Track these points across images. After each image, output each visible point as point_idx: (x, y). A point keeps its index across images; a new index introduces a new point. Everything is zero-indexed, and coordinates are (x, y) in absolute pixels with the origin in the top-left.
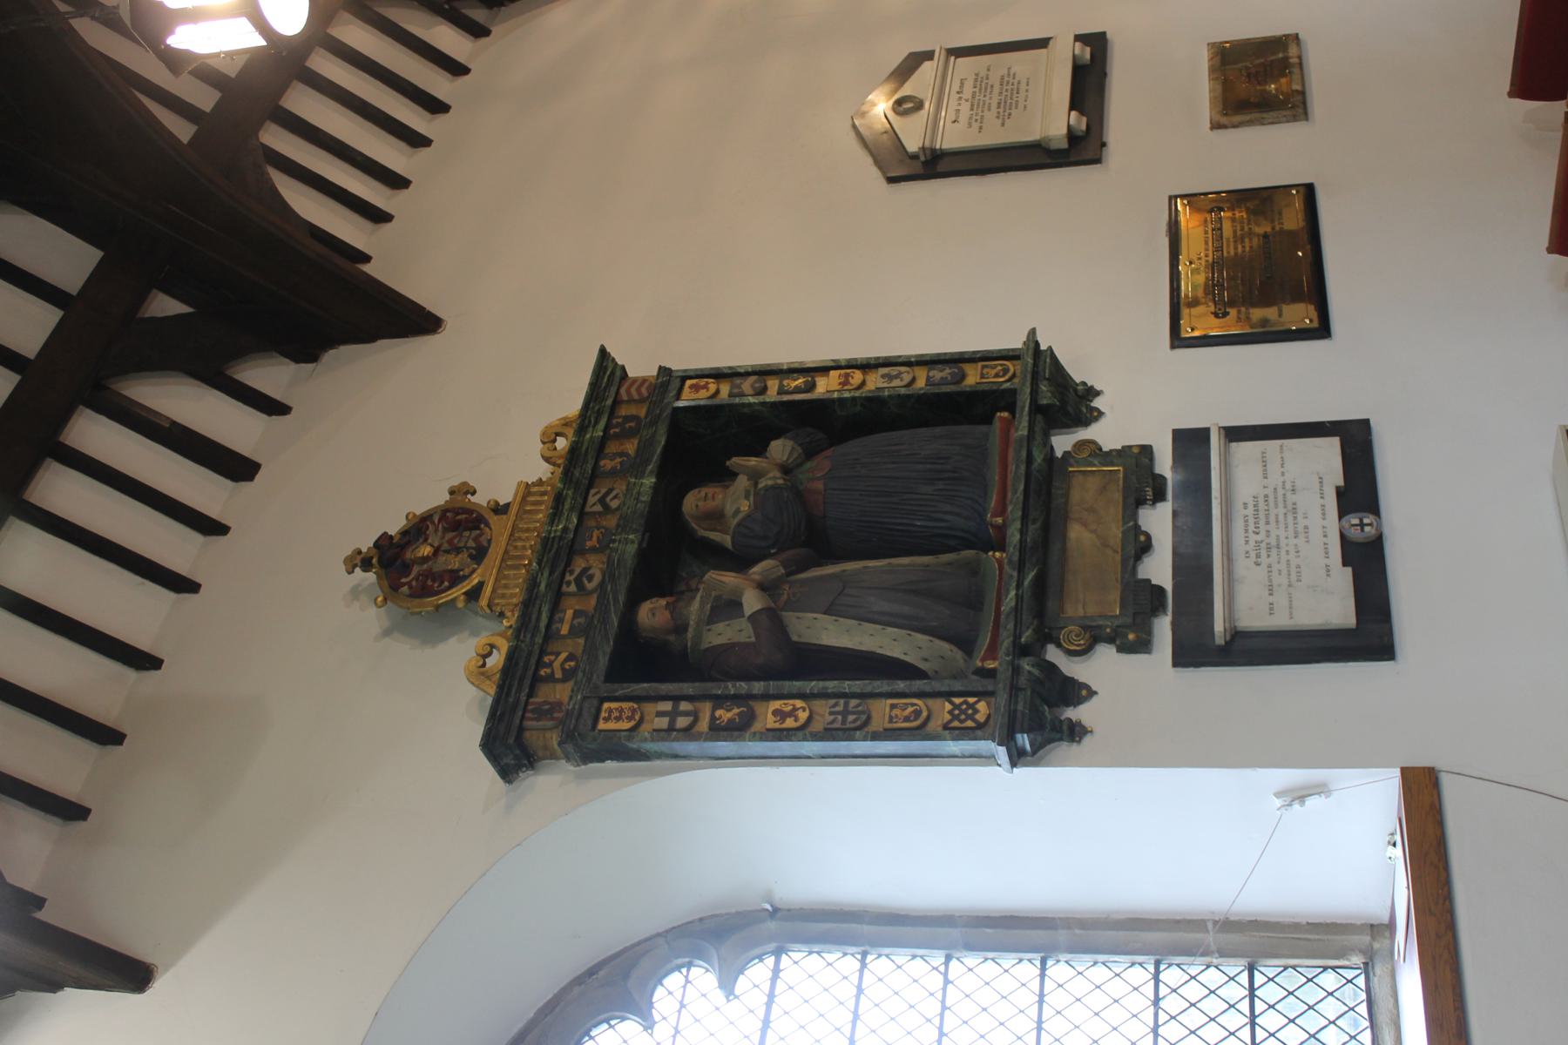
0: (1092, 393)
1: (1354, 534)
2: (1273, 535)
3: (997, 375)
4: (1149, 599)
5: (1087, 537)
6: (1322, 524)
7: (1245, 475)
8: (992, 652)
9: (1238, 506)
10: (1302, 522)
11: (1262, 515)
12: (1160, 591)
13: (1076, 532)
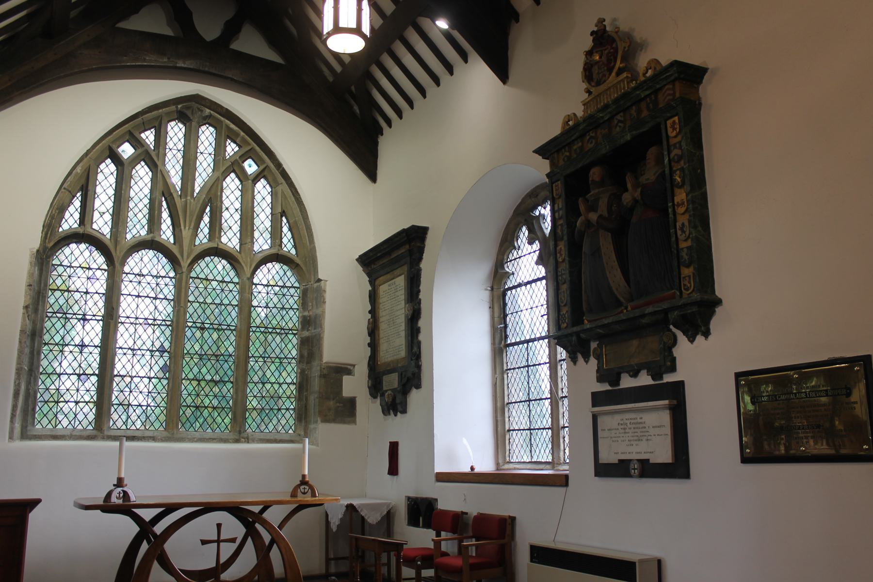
0: (707, 334)
1: (632, 466)
2: (630, 431)
3: (685, 285)
4: (615, 380)
5: (635, 349)
7: (656, 418)
8: (589, 321)
9: (641, 415)
10: (634, 443)
11: (638, 426)
12: (619, 385)
13: (635, 343)
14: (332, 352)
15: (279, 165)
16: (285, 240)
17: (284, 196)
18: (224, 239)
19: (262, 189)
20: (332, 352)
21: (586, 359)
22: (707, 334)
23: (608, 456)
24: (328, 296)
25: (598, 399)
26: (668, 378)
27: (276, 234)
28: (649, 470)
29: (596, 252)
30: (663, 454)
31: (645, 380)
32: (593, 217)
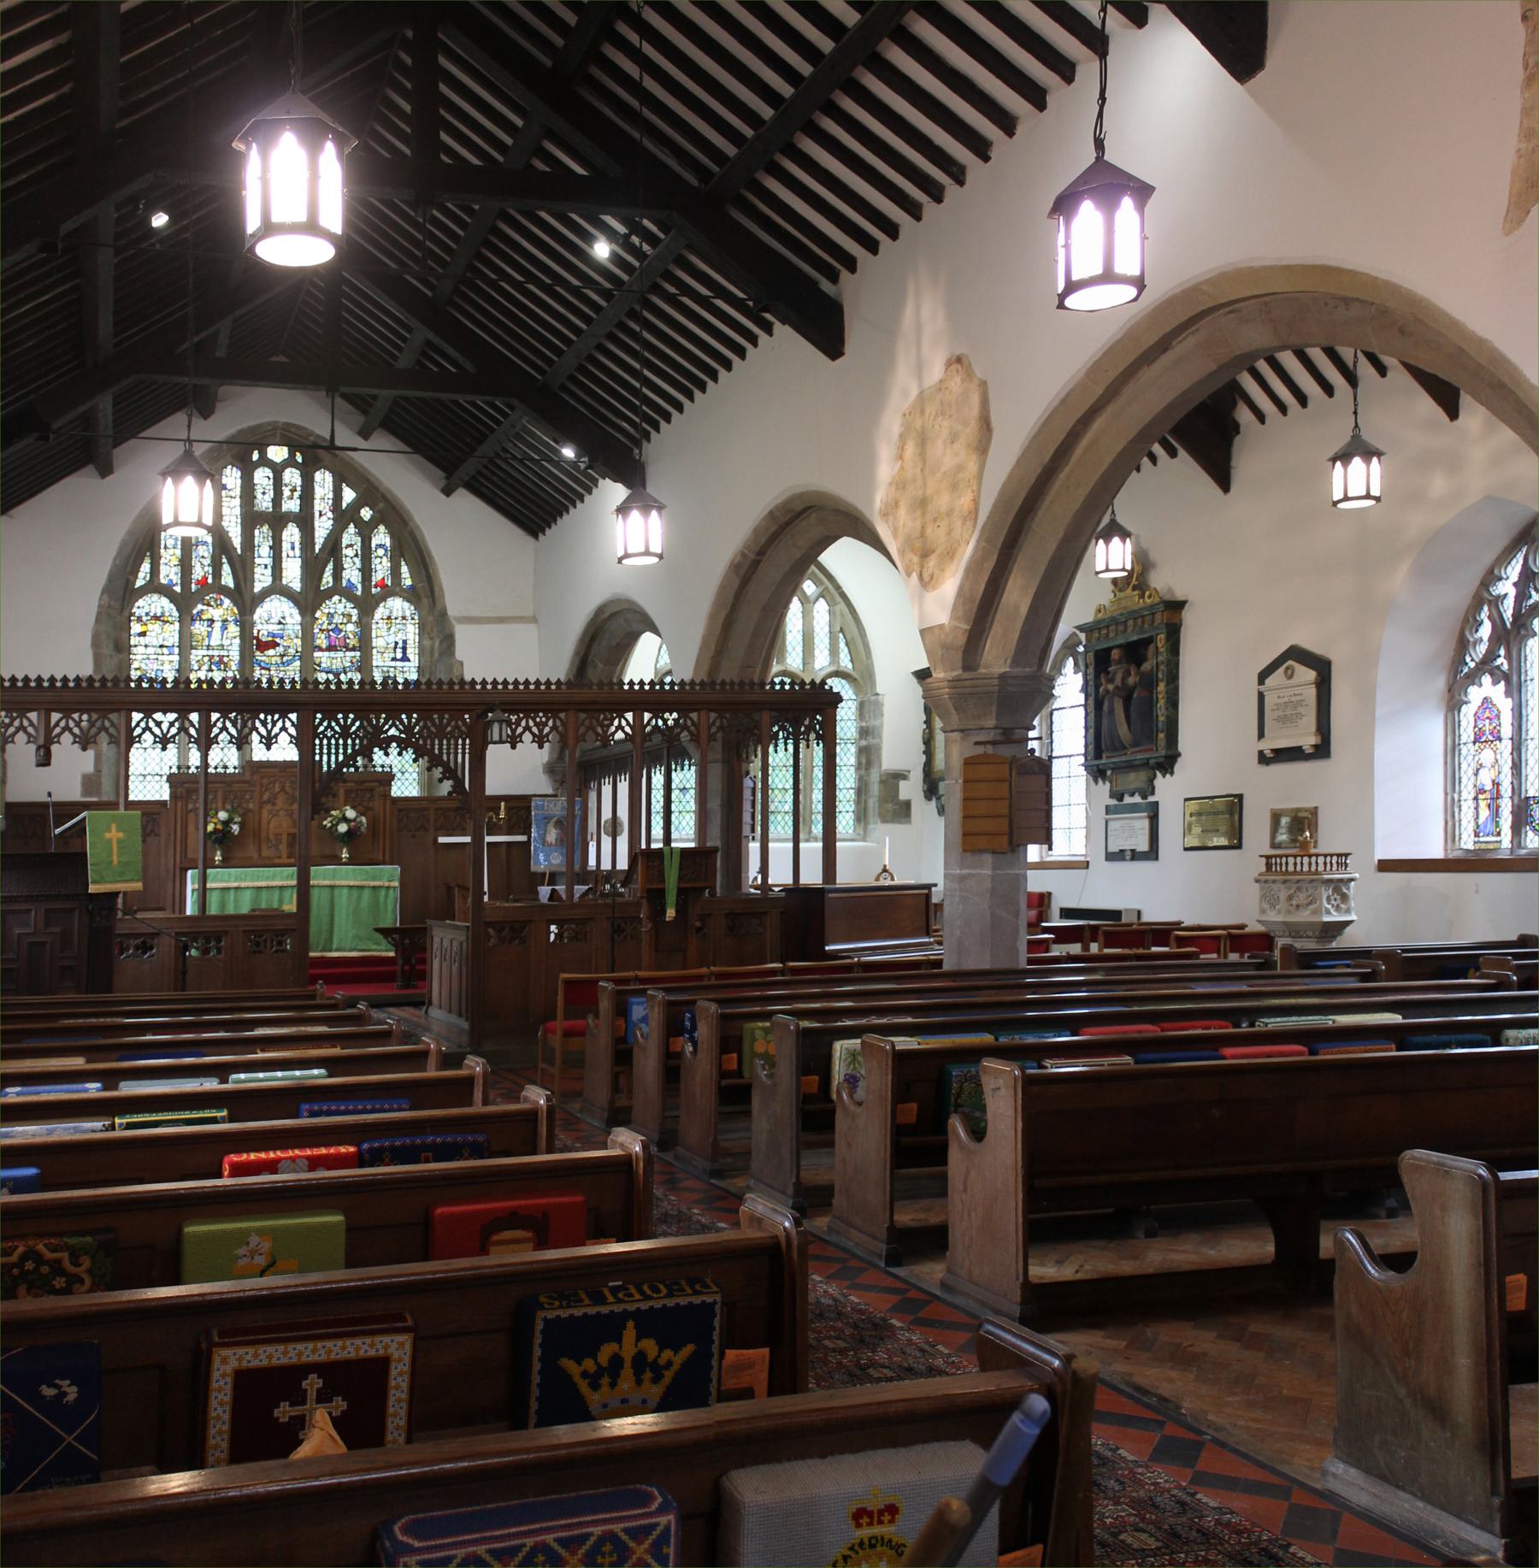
0: (1172, 773)
4: (1121, 799)
5: (1135, 779)
6: (1127, 845)
14: (890, 759)
15: (838, 588)
16: (842, 656)
17: (842, 615)
18: (789, 660)
19: (821, 607)
20: (890, 759)
21: (1104, 780)
22: (1172, 773)
23: (1113, 848)
24: (886, 710)
25: (1108, 810)
26: (1151, 799)
27: (834, 652)
28: (1135, 856)
29: (1112, 711)
30: (1143, 845)
31: (1137, 799)
32: (1111, 687)
